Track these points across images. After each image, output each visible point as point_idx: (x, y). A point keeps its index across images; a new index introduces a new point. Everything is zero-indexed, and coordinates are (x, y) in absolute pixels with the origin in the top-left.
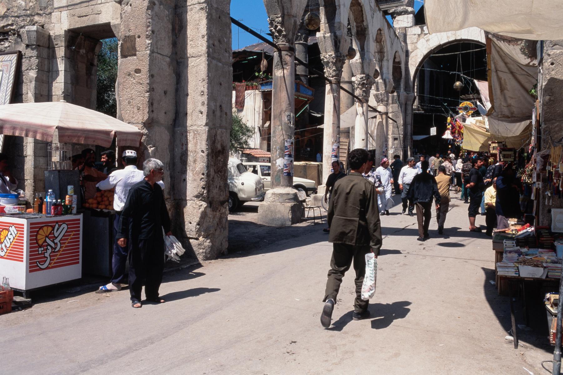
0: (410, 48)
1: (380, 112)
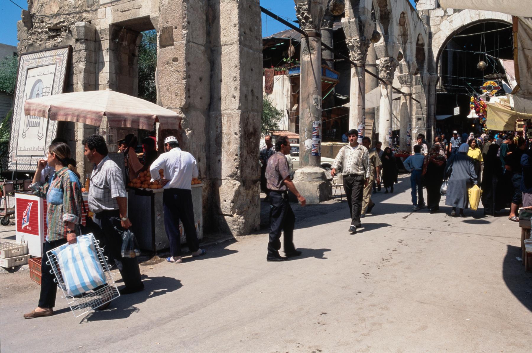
0: (433, 30)
1: (403, 93)
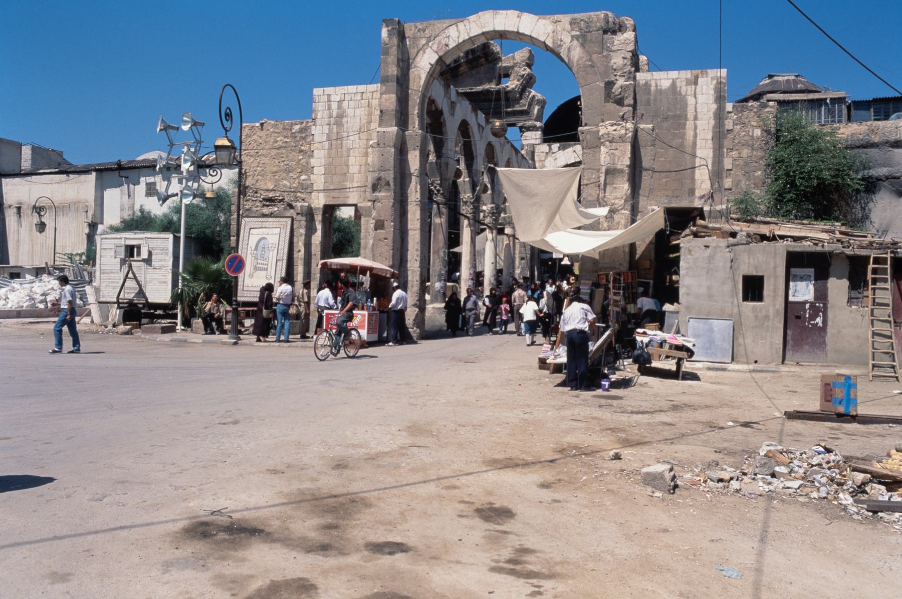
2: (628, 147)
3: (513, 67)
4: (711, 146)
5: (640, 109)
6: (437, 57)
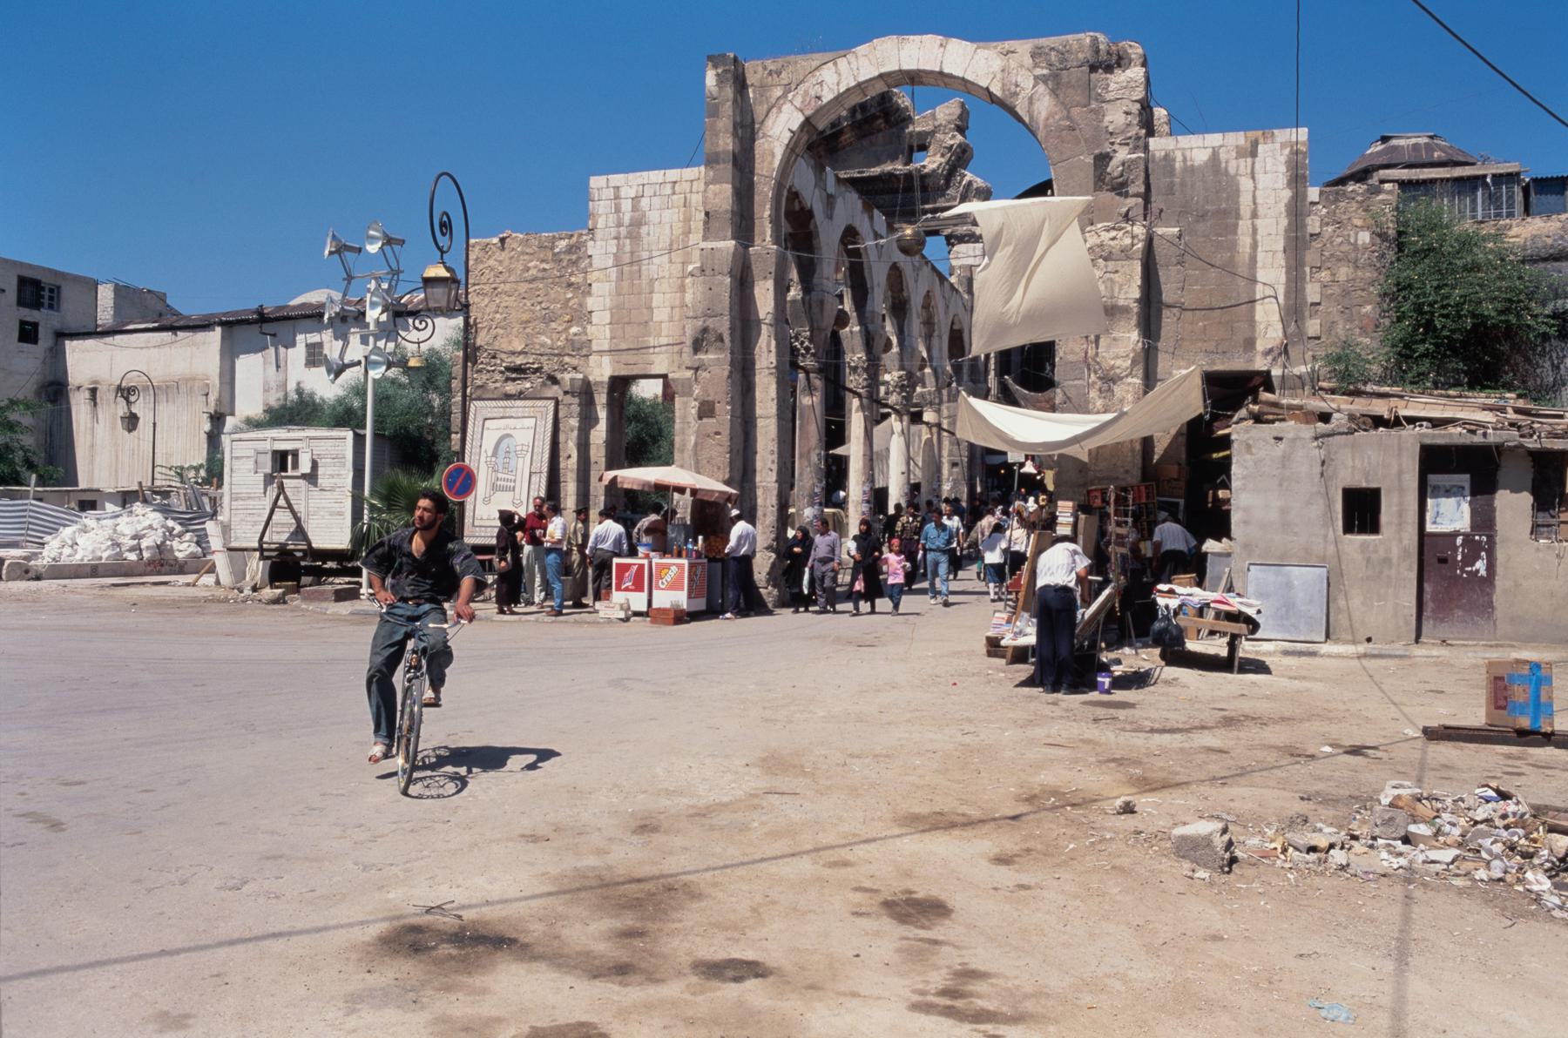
1: (927, 424)
2: (1137, 268)
3: (933, 133)
4: (1283, 263)
5: (1157, 202)
6: (802, 119)
